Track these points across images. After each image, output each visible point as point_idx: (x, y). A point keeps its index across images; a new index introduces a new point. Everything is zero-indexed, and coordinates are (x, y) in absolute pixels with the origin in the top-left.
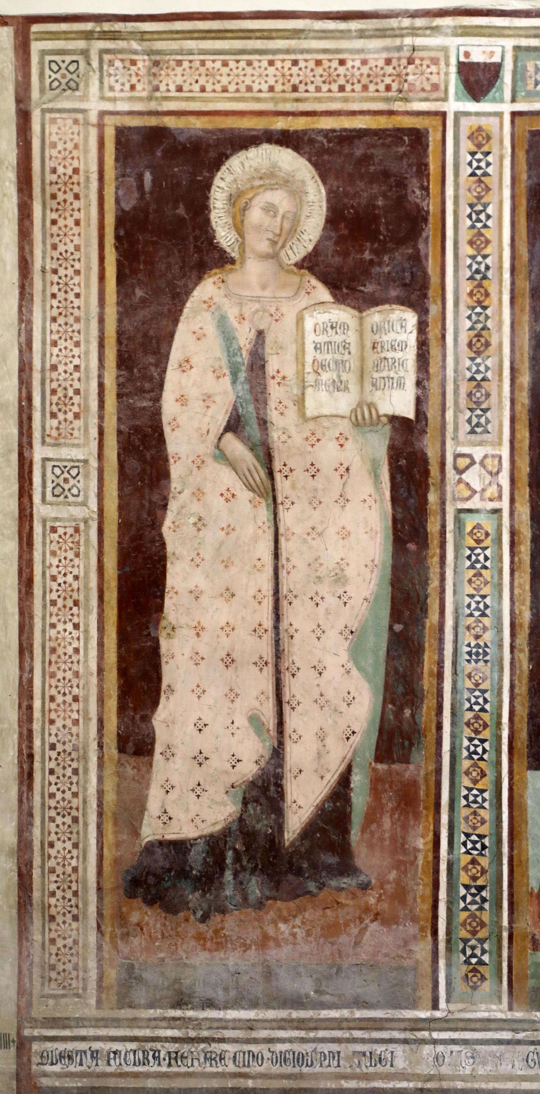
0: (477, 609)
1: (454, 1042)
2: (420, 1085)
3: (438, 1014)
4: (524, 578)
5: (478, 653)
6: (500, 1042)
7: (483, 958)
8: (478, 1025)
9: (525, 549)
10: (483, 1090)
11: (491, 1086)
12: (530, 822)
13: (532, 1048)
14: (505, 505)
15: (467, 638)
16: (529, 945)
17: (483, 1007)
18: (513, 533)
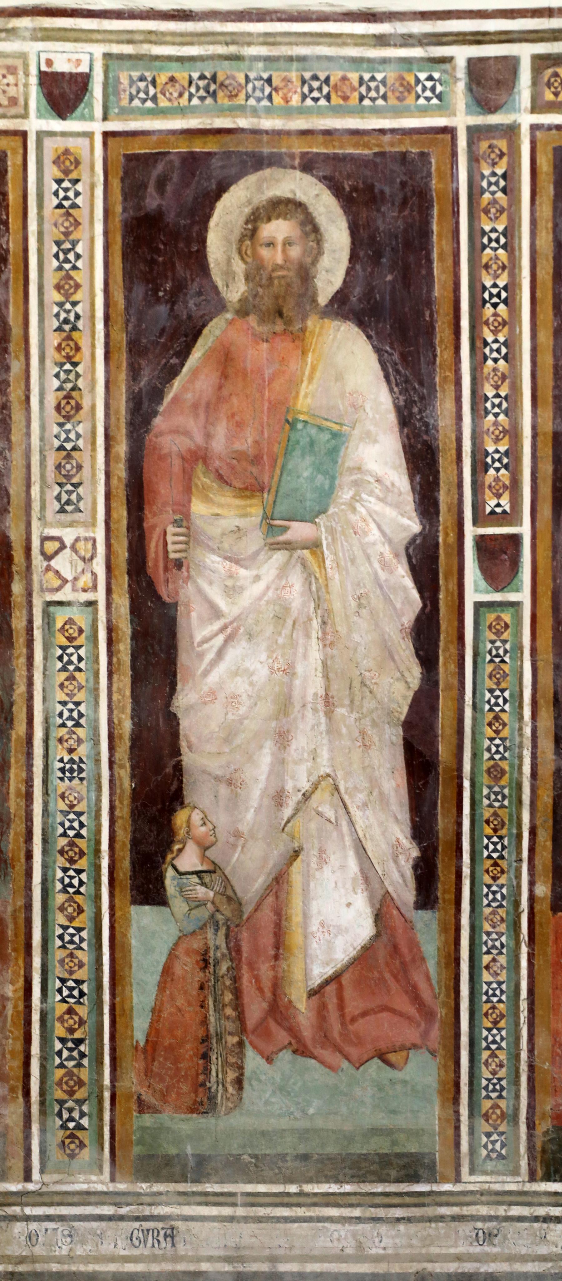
0: (71, 718)
1: (49, 1218)
2: (10, 1268)
3: (31, 1187)
4: (124, 681)
5: (73, 770)
6: (100, 1218)
7: (82, 1122)
8: (76, 1199)
9: (125, 648)
10: (82, 1273)
11: (91, 1268)
12: (134, 965)
13: (137, 1224)
14: (101, 596)
15: (59, 752)
16: (134, 1107)
17: (82, 1178)
18: (110, 630)
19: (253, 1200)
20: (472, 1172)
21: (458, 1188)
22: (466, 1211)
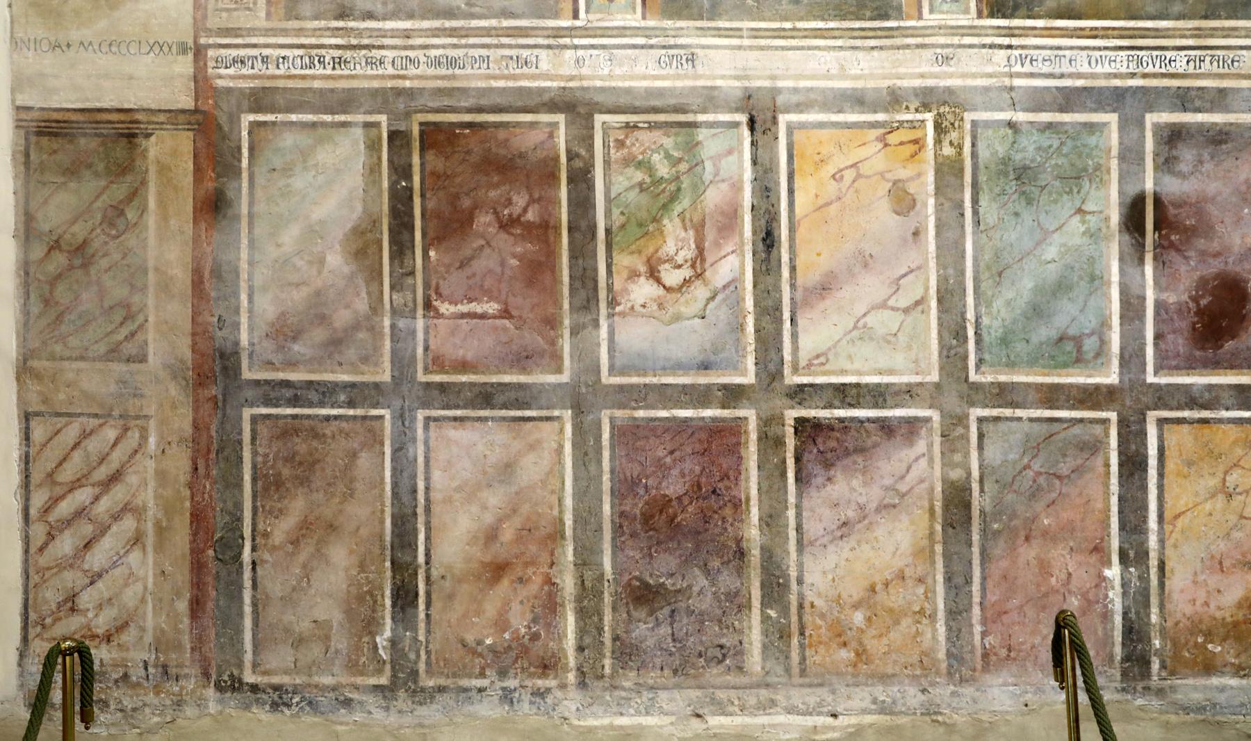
1: (593, 47)
2: (562, 84)
3: (578, 23)
6: (635, 47)
8: (615, 32)
10: (620, 88)
11: (627, 84)
13: (664, 52)
17: (619, 16)
19: (756, 33)
20: (931, 11)
21: (921, 23)
22: (927, 40)
